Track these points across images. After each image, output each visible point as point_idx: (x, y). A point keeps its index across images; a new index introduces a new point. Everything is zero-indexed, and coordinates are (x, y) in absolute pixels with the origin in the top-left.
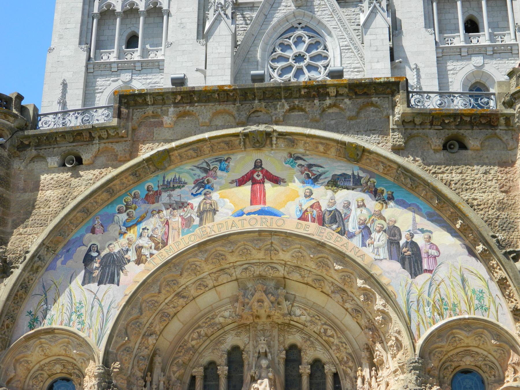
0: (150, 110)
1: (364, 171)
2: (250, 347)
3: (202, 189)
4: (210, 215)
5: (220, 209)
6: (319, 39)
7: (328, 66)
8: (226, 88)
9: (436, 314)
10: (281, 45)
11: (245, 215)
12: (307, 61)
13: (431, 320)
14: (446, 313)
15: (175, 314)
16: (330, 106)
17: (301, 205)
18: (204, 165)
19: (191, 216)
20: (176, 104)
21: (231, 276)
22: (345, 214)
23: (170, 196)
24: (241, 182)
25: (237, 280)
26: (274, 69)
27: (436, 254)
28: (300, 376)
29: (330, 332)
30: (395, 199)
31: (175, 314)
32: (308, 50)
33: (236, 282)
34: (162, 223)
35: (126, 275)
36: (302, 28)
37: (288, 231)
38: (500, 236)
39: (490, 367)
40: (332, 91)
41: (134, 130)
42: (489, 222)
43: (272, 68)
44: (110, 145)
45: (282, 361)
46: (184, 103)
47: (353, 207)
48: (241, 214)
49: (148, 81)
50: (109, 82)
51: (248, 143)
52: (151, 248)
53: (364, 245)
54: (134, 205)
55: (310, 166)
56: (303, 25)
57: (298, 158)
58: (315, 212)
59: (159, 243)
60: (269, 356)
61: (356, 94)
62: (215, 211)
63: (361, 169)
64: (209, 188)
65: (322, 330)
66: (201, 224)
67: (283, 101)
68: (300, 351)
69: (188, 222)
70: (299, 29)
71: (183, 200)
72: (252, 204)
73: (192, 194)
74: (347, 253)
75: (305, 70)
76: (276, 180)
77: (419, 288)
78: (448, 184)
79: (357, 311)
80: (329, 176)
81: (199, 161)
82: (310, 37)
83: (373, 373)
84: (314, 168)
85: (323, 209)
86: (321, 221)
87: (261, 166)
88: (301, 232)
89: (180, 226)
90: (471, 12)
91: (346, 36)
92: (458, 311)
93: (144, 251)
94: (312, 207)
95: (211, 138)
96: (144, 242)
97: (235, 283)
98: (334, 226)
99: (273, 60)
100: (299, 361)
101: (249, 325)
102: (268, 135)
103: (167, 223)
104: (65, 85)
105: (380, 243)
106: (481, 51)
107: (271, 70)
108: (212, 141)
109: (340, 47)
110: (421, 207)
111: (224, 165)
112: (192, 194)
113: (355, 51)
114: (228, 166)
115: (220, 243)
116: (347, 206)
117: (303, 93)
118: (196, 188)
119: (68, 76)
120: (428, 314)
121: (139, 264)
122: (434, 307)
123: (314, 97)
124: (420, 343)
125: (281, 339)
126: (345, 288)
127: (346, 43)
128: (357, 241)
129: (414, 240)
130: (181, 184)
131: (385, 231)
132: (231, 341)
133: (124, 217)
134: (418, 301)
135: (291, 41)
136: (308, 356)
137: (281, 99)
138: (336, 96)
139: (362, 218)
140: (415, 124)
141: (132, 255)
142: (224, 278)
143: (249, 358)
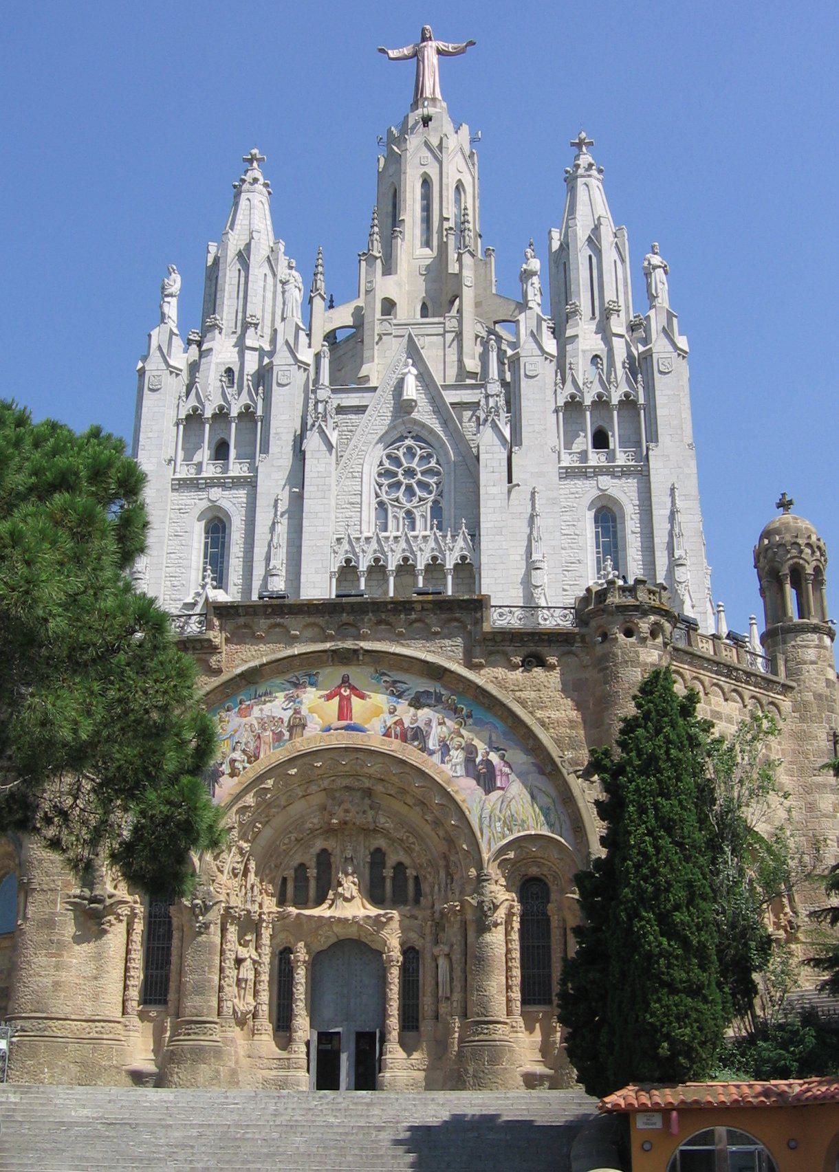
0: (242, 621)
1: (446, 688)
2: (337, 851)
3: (292, 703)
4: (299, 730)
5: (309, 724)
8: (315, 602)
9: (506, 829)
11: (332, 731)
12: (419, 476)
13: (500, 835)
14: (515, 828)
15: (267, 822)
16: (416, 621)
17: (385, 722)
18: (294, 680)
19: (281, 731)
20: (267, 616)
21: (320, 787)
22: (427, 732)
23: (261, 710)
24: (329, 697)
25: (325, 790)
26: (380, 486)
27: (509, 772)
28: (384, 878)
29: (412, 840)
30: (474, 717)
31: (267, 822)
33: (324, 792)
34: (255, 736)
35: (221, 787)
36: (412, 437)
37: (373, 748)
39: (554, 877)
40: (418, 607)
42: (558, 742)
43: (378, 484)
44: (204, 656)
45: (367, 865)
46: (275, 615)
47: (434, 724)
48: (328, 729)
51: (336, 659)
52: (244, 761)
53: (443, 762)
54: (227, 719)
55: (395, 682)
57: (384, 674)
58: (398, 728)
59: (251, 757)
60: (355, 861)
61: (441, 609)
62: (304, 726)
63: (444, 686)
64: (298, 702)
65: (405, 838)
66: (291, 738)
67: (370, 614)
68: (384, 854)
69: (278, 737)
71: (273, 715)
72: (339, 720)
73: (283, 709)
74: (427, 771)
76: (362, 697)
77: (492, 804)
78: (523, 703)
79: (437, 823)
80: (412, 693)
81: (287, 677)
82: (421, 449)
83: (449, 881)
84: (399, 685)
85: (406, 726)
86: (404, 737)
87: (348, 681)
88: (384, 748)
89: (271, 741)
90: (601, 423)
92: (526, 826)
93: (236, 764)
94: (395, 723)
95: (300, 655)
96: (237, 755)
97: (324, 793)
98: (416, 743)
100: (383, 864)
101: (336, 830)
102: (355, 651)
103: (259, 737)
105: (458, 760)
107: (377, 487)
108: (301, 657)
110: (498, 725)
111: (313, 679)
112: (283, 709)
114: (317, 681)
115: (309, 758)
116: (429, 723)
117: (389, 607)
118: (286, 703)
120: (499, 829)
121: (232, 777)
122: (505, 822)
123: (400, 611)
125: (367, 844)
126: (425, 801)
128: (436, 758)
129: (489, 758)
131: (463, 749)
132: (319, 844)
134: (490, 817)
136: (392, 860)
137: (368, 612)
138: (423, 609)
139: (442, 736)
140: (496, 642)
141: (225, 768)
142: (314, 788)
143: (336, 860)
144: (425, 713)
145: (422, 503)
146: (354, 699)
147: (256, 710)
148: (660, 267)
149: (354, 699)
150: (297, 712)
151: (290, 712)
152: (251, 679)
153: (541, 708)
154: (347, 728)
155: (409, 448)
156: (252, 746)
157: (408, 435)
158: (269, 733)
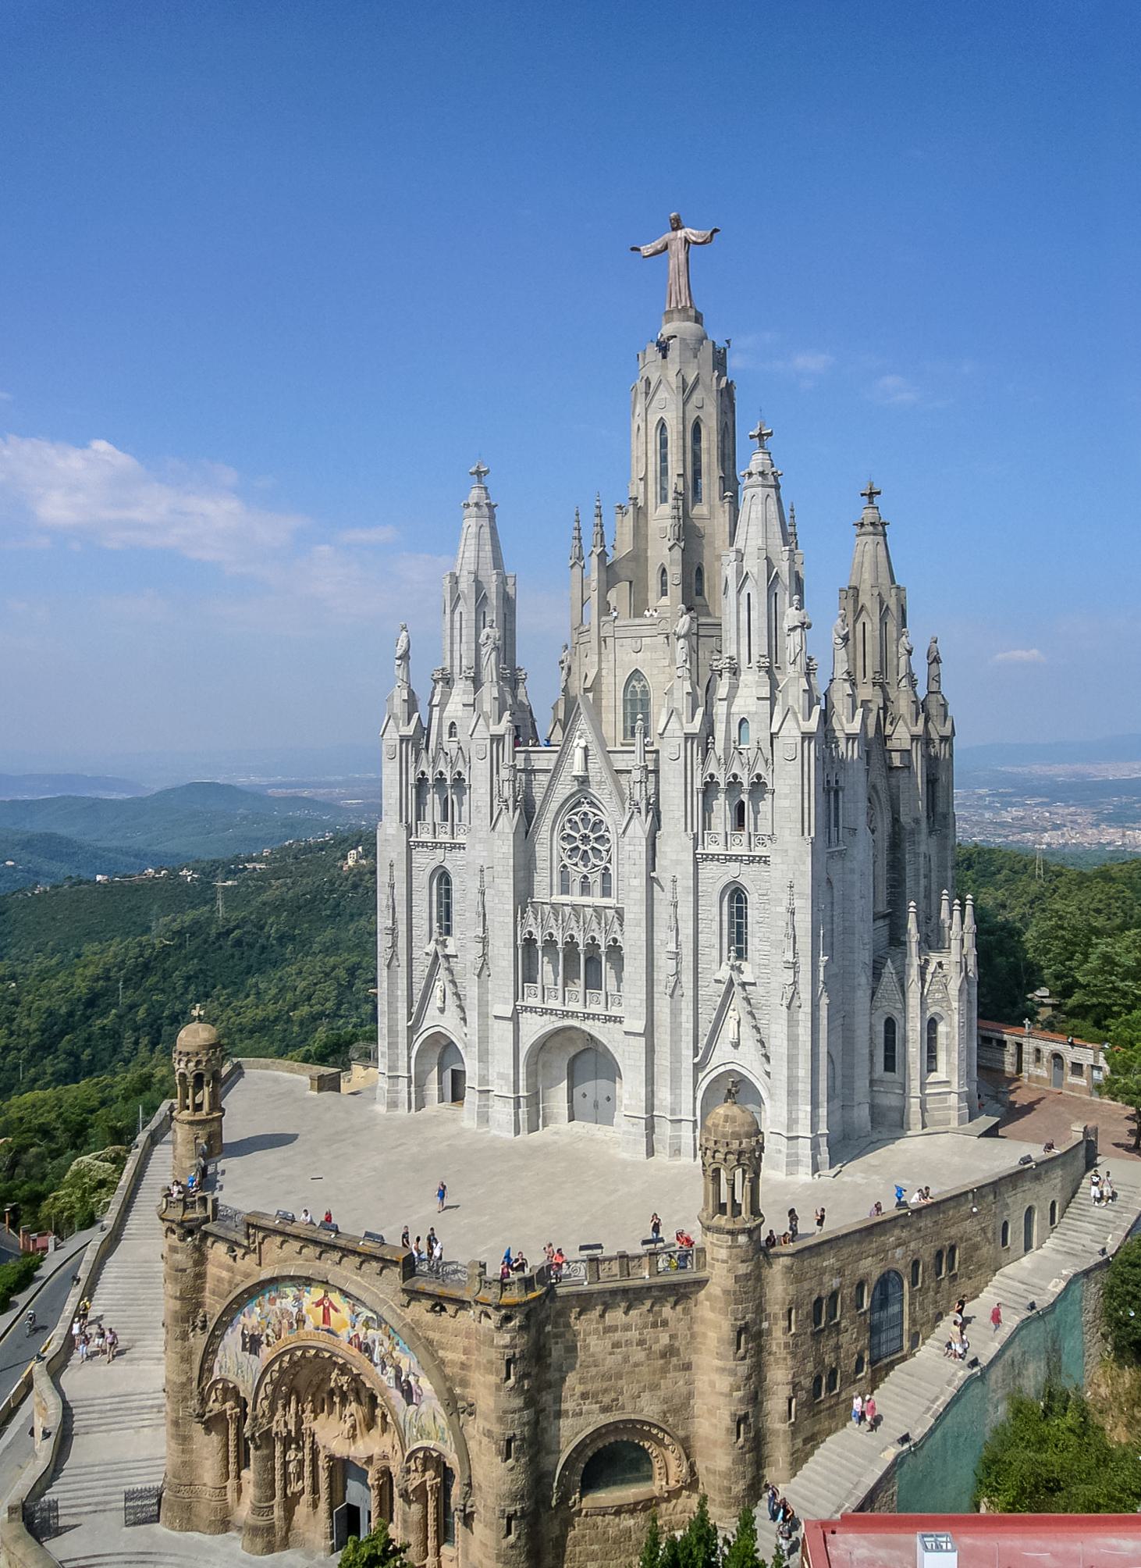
6: (602, 817)
10: (570, 821)
38: (458, 1390)
41: (260, 1244)
47: (377, 1344)
69: (291, 1325)
75: (590, 852)
76: (336, 1310)
96: (269, 1331)
103: (280, 1323)
104: (391, 866)
106: (737, 858)
116: (374, 1342)
119: (394, 856)
124: (407, 1454)
130: (287, 1297)
133: (258, 1310)
144: (370, 1331)
146: (331, 1310)
147: (278, 1301)
149: (331, 1310)
150: (300, 1310)
151: (296, 1309)
152: (274, 1281)
153: (443, 1349)
154: (328, 1331)
155: (585, 814)
156: (277, 1330)
158: (285, 1321)
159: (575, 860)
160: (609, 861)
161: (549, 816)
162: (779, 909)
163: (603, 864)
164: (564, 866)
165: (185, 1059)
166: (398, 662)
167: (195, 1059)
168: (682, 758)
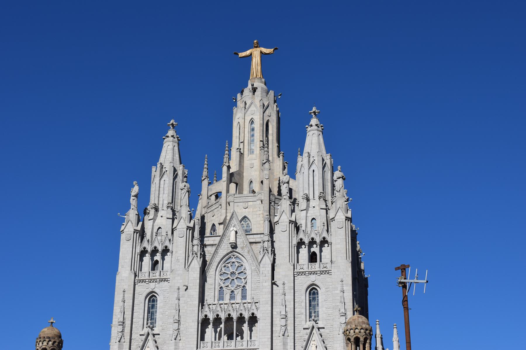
7: (246, 278)
32: (236, 270)
36: (235, 258)
49: (163, 289)
50: (145, 289)
56: (235, 256)
70: (234, 259)
75: (235, 280)
91: (254, 264)
99: (221, 275)
106: (315, 273)
109: (251, 270)
113: (258, 272)
119: (126, 287)
127: (254, 268)
135: (229, 265)
145: (238, 287)
148: (341, 177)
155: (233, 262)
157: (234, 257)
159: (227, 285)
160: (246, 282)
161: (215, 264)
162: (336, 292)
163: (243, 285)
164: (221, 288)
165: (47, 340)
166: (134, 198)
167: (53, 340)
168: (288, 231)
